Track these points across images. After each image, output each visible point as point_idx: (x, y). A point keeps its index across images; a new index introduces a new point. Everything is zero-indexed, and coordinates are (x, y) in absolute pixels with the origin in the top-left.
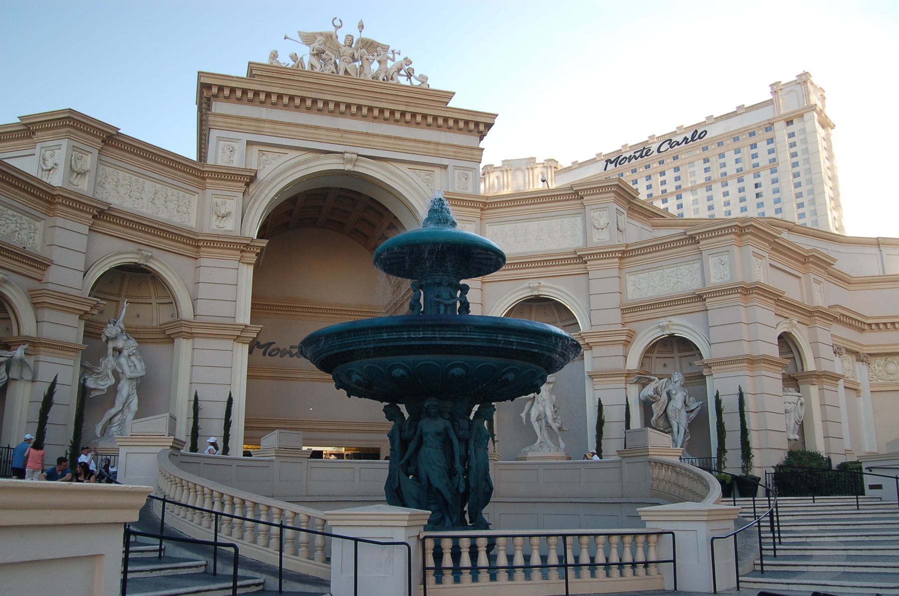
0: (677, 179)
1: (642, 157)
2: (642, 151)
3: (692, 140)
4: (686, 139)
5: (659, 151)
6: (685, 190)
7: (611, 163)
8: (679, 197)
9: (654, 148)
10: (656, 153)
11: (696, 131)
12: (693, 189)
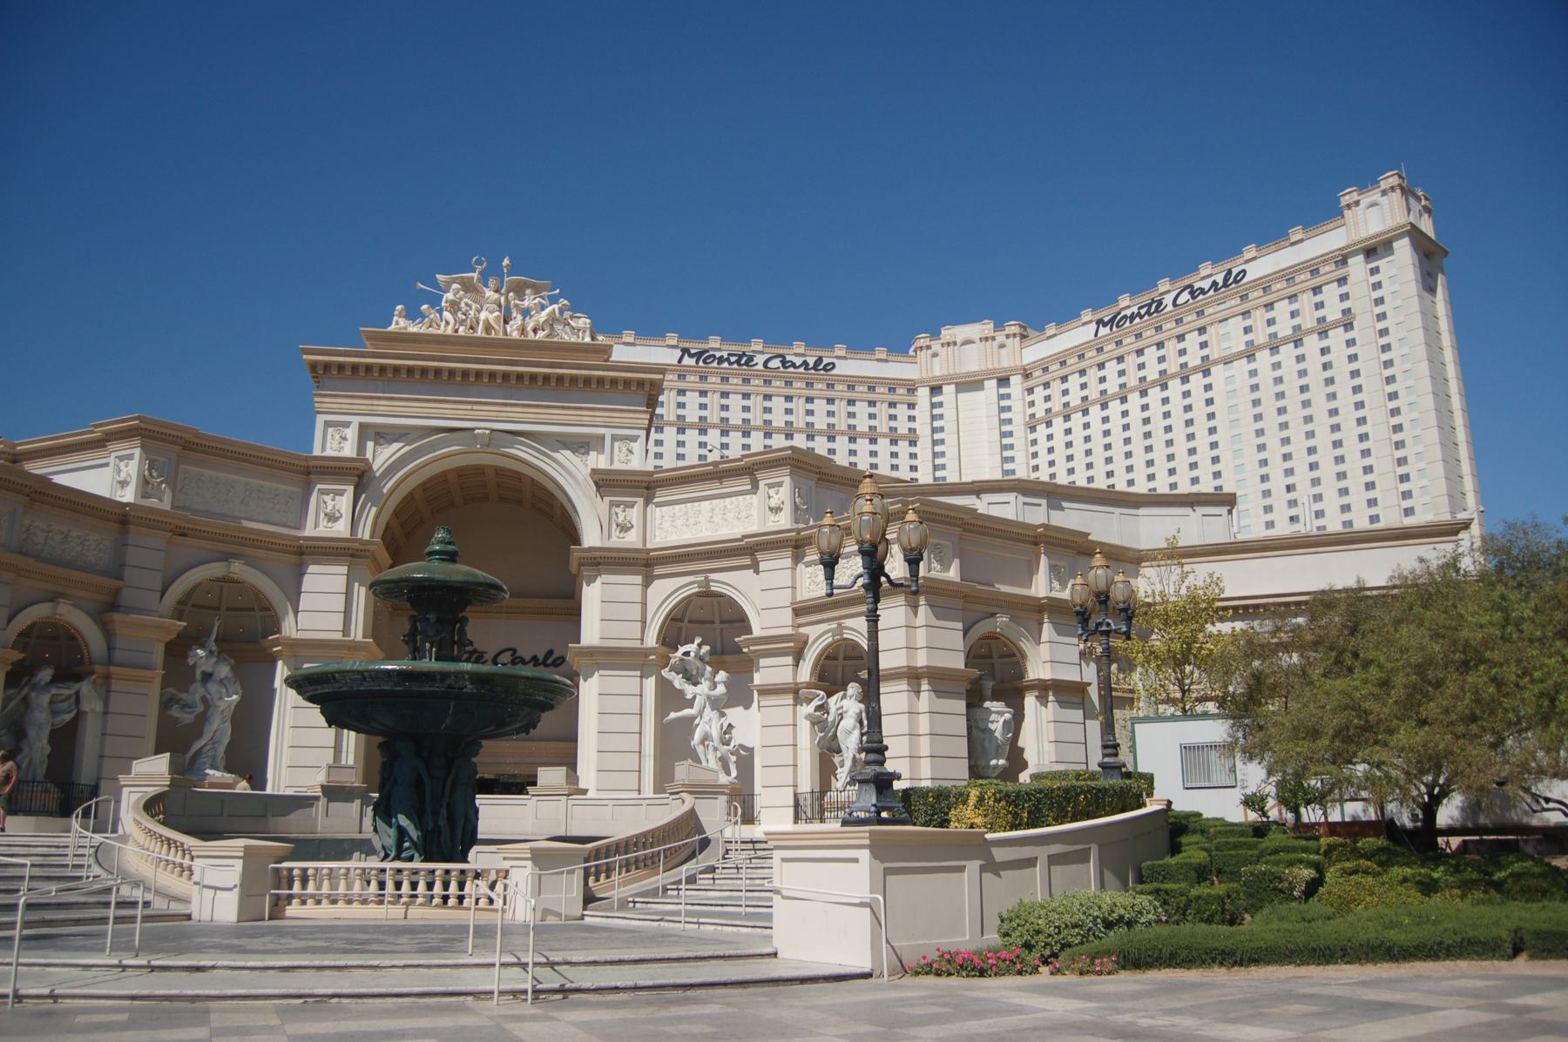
0: (1204, 345)
2: (1150, 305)
3: (1225, 285)
4: (1215, 284)
5: (1175, 304)
6: (1216, 363)
7: (1105, 325)
8: (1206, 373)
9: (1168, 300)
10: (1170, 308)
11: (1229, 272)
12: (1227, 361)
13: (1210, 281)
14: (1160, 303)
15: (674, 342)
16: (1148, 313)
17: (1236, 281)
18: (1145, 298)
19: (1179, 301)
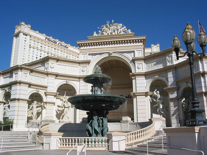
2: (55, 41)
3: (65, 47)
4: (64, 46)
5: (58, 44)
7: (47, 39)
9: (58, 43)
10: (57, 44)
13: (64, 45)
14: (56, 42)
15: (45, 36)
16: (54, 42)
17: (67, 47)
18: (55, 40)
19: (59, 44)
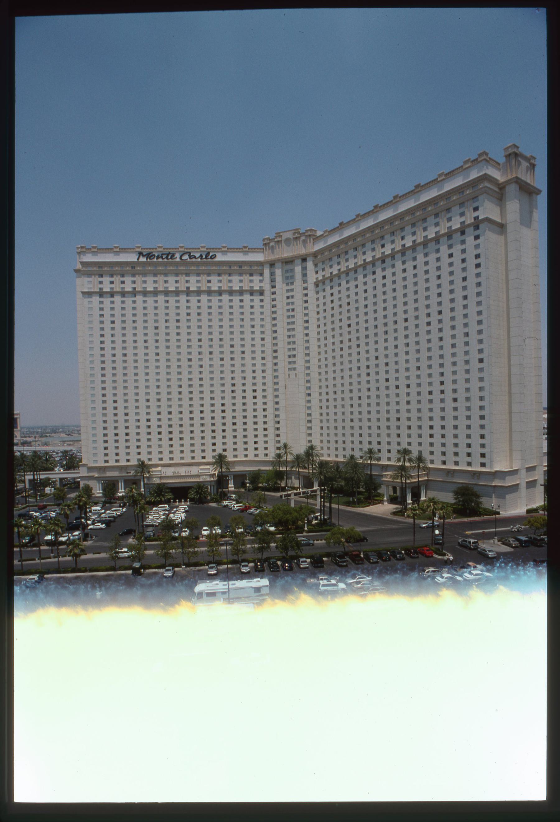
1: (168, 259)
2: (168, 255)
3: (206, 258)
5: (181, 258)
9: (177, 255)
10: (178, 259)
11: (209, 253)
14: (173, 255)
17: (211, 258)
19: (183, 258)
